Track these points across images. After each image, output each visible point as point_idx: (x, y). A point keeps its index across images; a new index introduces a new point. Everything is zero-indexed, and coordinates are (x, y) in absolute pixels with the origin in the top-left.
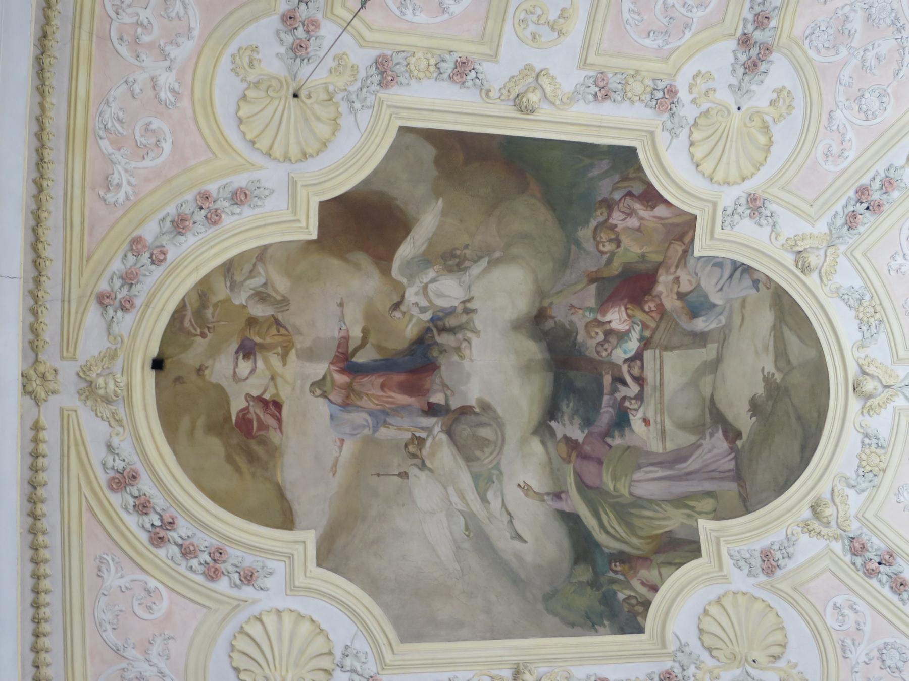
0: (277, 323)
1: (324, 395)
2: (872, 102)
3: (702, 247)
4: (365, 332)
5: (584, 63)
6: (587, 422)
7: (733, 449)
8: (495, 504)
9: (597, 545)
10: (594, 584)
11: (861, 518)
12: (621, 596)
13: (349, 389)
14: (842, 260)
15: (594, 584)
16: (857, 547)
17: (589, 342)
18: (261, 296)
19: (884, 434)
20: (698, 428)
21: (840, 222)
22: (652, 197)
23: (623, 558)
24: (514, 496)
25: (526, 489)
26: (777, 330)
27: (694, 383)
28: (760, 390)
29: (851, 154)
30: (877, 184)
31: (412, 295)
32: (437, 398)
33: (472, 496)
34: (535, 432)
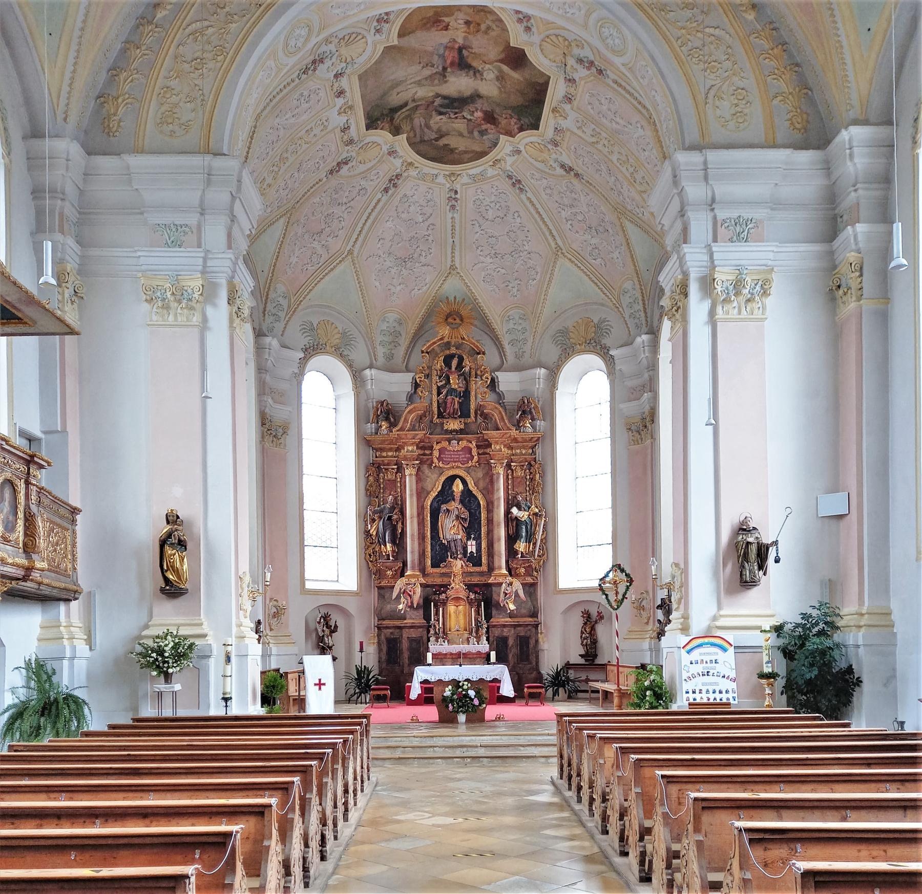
0: (478, 31)
1: (450, 42)
2: (548, 191)
3: (503, 138)
4: (474, 53)
5: (568, 130)
6: (441, 106)
7: (432, 140)
8: (409, 87)
9: (396, 112)
10: (382, 115)
11: (408, 176)
12: (379, 122)
13: (452, 48)
14: (497, 172)
15: (382, 115)
16: (398, 176)
17: (471, 107)
20: (439, 130)
21: (510, 174)
22: (521, 129)
23: (392, 120)
24: (413, 91)
25: (416, 93)
26: (473, 151)
27: (454, 130)
28: (452, 147)
29: (532, 181)
30: (521, 187)
31: (487, 66)
32: (449, 70)
33: (413, 80)
34: (437, 94)
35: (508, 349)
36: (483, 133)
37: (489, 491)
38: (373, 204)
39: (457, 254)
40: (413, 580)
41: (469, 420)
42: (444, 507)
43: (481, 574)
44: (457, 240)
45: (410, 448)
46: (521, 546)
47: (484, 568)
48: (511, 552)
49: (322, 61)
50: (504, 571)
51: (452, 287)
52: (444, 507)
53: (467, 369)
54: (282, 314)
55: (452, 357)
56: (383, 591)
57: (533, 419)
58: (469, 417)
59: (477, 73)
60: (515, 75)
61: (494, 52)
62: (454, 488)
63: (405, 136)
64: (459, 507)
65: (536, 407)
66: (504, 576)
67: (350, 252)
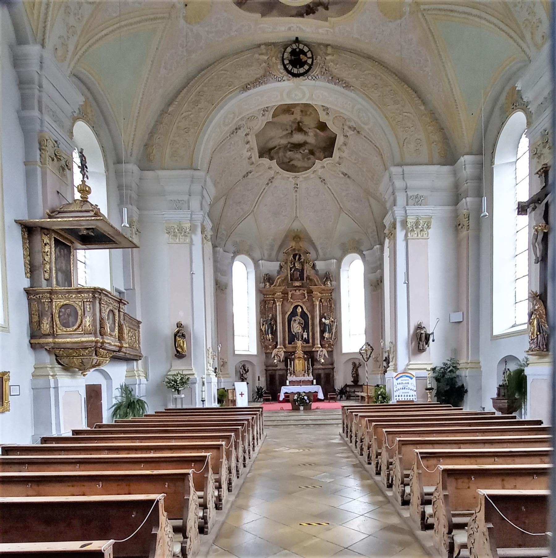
17: (303, 148)
18: (311, 113)
19: (289, 180)
26: (305, 167)
31: (310, 130)
35: (320, 251)
36: (309, 159)
37: (312, 311)
38: (262, 190)
39: (298, 211)
40: (280, 350)
41: (303, 282)
42: (293, 319)
43: (310, 347)
44: (298, 205)
45: (279, 294)
46: (326, 335)
47: (310, 344)
48: (322, 338)
49: (240, 129)
50: (319, 346)
51: (296, 226)
52: (293, 319)
53: (303, 260)
54: (224, 238)
55: (296, 254)
56: (268, 355)
57: (331, 281)
58: (304, 280)
59: (306, 133)
60: (321, 134)
61: (313, 124)
62: (298, 310)
63: (275, 160)
64: (300, 318)
65: (332, 276)
66: (319, 348)
67: (253, 211)
